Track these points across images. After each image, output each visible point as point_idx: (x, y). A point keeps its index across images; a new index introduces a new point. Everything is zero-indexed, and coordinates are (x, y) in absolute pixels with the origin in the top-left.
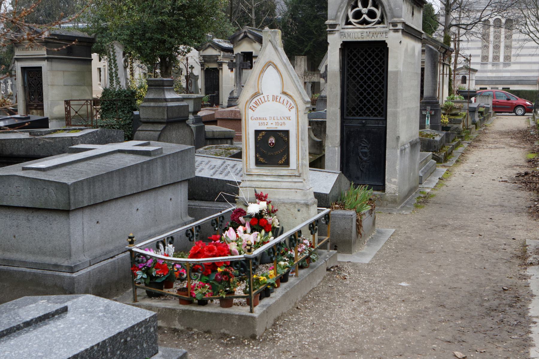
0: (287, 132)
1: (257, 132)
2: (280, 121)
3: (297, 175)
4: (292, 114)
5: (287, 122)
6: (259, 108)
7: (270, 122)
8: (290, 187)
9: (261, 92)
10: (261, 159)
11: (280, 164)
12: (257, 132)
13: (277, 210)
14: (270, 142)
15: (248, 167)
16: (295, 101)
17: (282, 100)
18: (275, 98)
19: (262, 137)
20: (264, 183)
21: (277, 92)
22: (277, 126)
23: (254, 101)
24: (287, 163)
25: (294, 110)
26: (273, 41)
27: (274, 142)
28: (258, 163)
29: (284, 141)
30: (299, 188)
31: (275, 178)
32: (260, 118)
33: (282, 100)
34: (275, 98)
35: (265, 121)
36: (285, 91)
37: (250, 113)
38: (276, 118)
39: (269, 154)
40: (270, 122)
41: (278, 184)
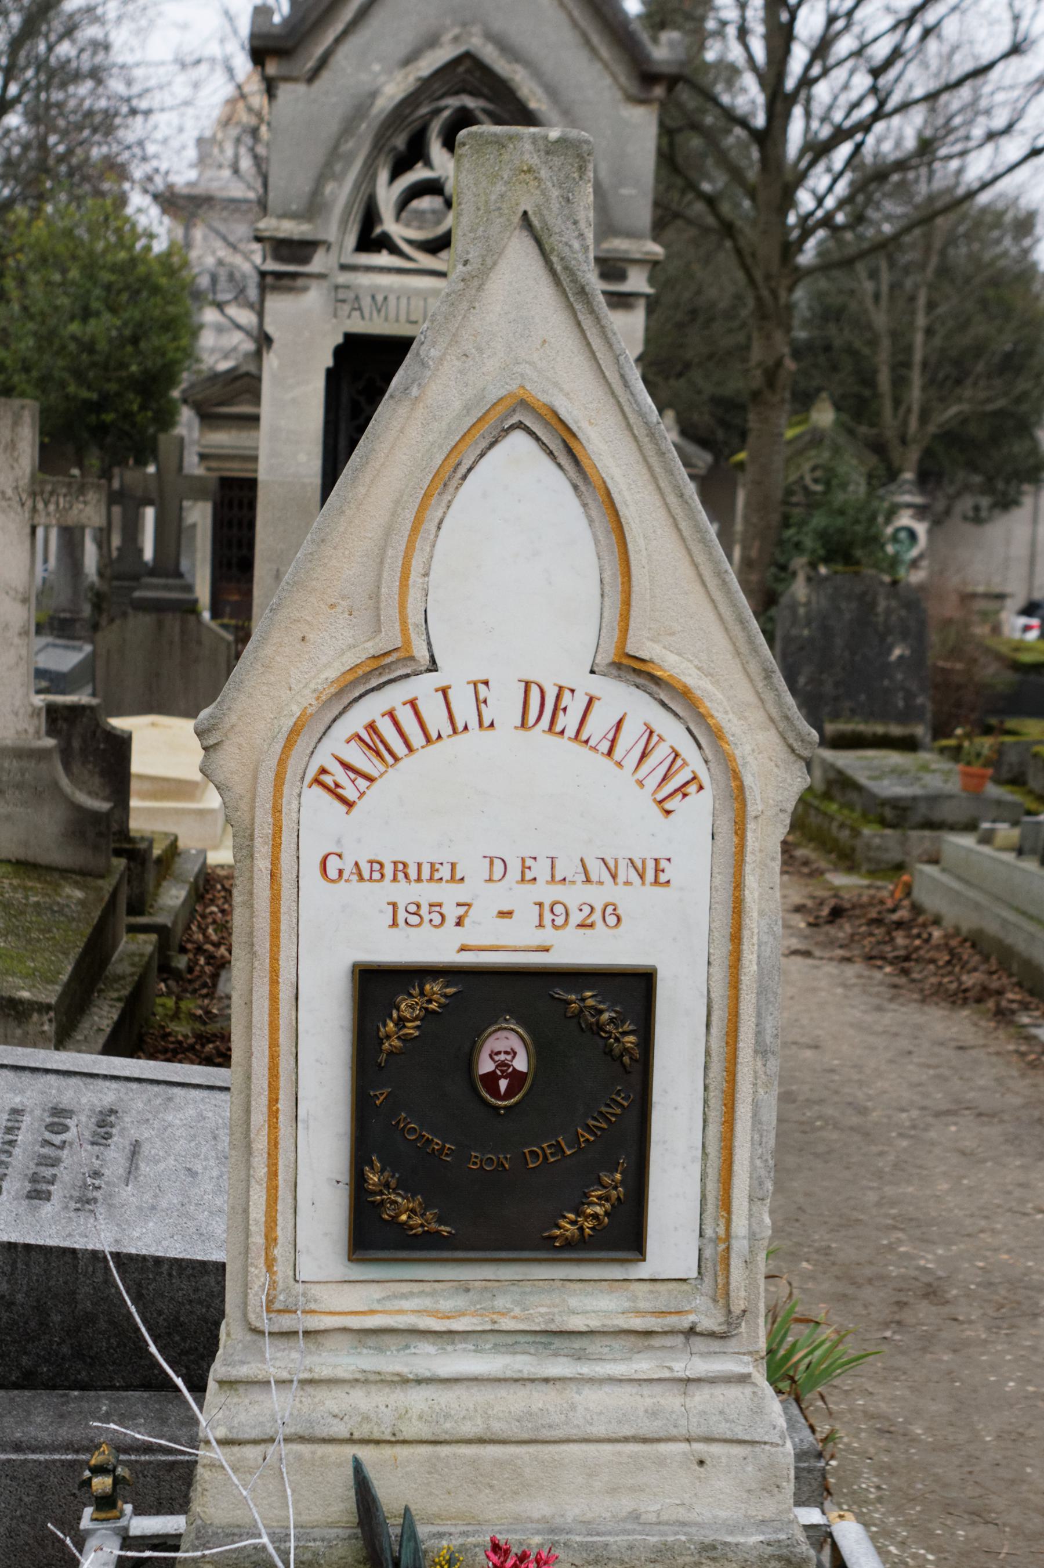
0: (636, 988)
1: (376, 987)
2: (575, 896)
3: (706, 1323)
4: (690, 836)
5: (634, 898)
6: (396, 784)
7: (488, 899)
8: (649, 1427)
9: (421, 653)
10: (405, 1209)
11: (569, 1245)
12: (376, 987)
13: (407, 1509)
14: (486, 1066)
15: (282, 1269)
16: (716, 734)
17: (598, 726)
18: (543, 708)
19: (413, 1027)
20: (417, 1399)
21: (564, 648)
22: (547, 935)
23: (355, 720)
24: (624, 1234)
25: (699, 810)
26: (556, 223)
27: (521, 1064)
28: (372, 1234)
29: (453, 1003)
30: (722, 1429)
31: (511, 1349)
32: (401, 869)
33: (598, 726)
34: (543, 708)
35: (448, 895)
36: (643, 646)
37: (317, 819)
38: (541, 870)
39: (476, 1160)
40: (488, 899)
41: (540, 1399)
